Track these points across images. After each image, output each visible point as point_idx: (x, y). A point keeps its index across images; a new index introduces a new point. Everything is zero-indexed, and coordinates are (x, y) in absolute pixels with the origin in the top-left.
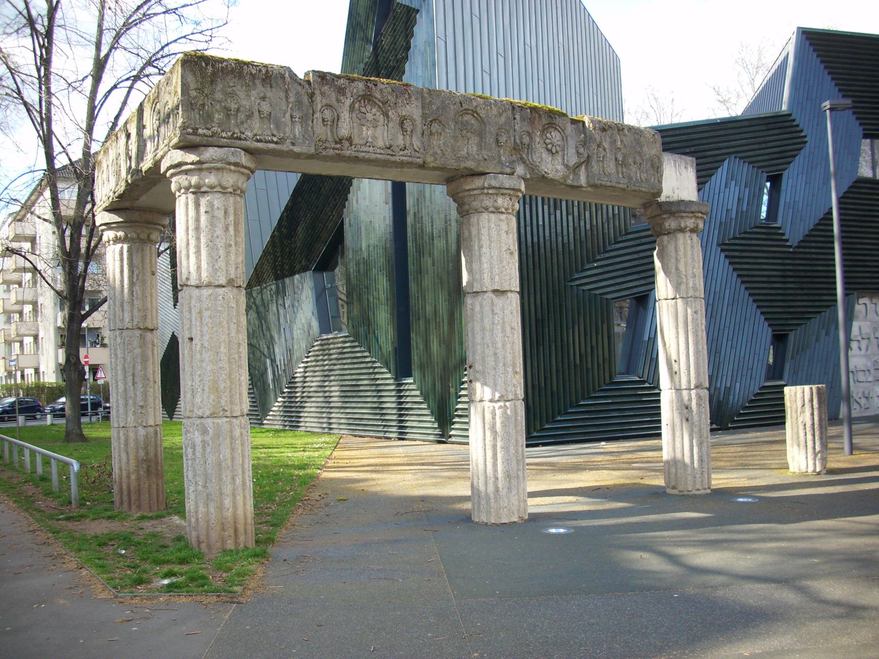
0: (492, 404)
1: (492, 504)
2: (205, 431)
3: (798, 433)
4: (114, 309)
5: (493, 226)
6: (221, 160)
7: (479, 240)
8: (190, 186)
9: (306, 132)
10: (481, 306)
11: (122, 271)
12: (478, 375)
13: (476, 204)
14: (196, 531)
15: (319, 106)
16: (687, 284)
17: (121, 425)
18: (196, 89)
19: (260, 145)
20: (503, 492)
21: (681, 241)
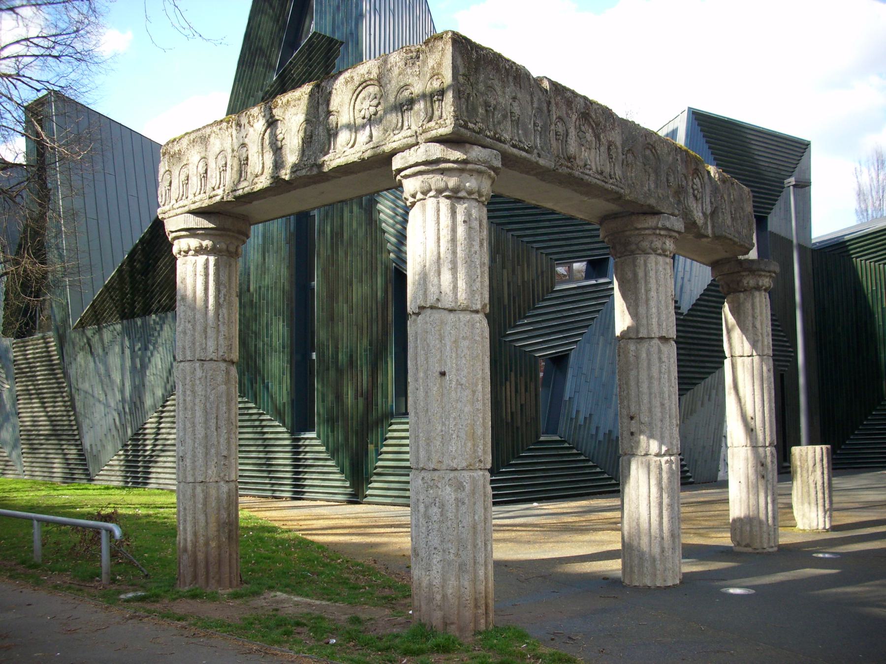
0: (658, 459)
1: (658, 567)
2: (460, 487)
3: (808, 492)
4: (193, 335)
5: (661, 269)
6: (484, 162)
7: (647, 282)
8: (446, 189)
9: (545, 144)
10: (648, 353)
11: (206, 289)
12: (643, 427)
13: (645, 244)
14: (441, 610)
15: (555, 117)
16: (763, 342)
17: (200, 479)
18: (463, 75)
19: (515, 151)
20: (668, 553)
21: (757, 300)
